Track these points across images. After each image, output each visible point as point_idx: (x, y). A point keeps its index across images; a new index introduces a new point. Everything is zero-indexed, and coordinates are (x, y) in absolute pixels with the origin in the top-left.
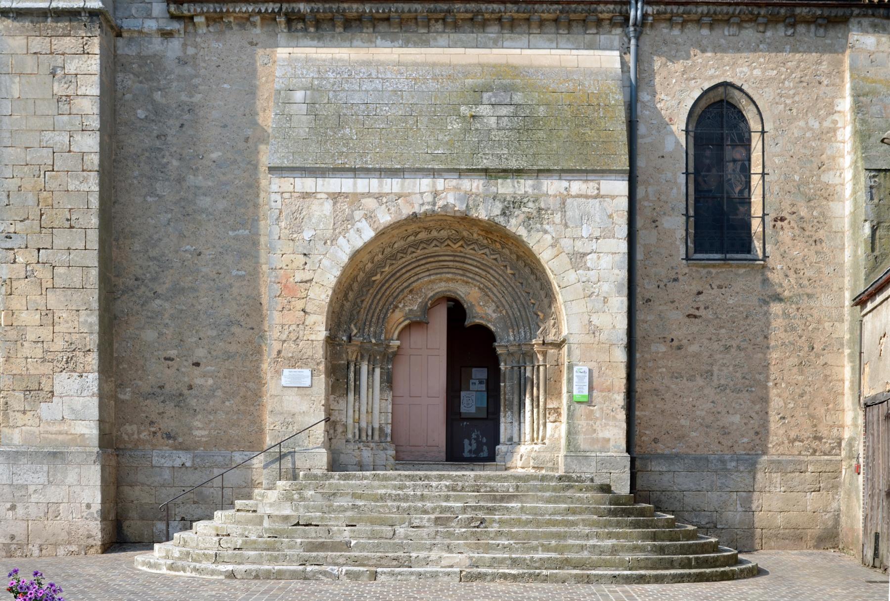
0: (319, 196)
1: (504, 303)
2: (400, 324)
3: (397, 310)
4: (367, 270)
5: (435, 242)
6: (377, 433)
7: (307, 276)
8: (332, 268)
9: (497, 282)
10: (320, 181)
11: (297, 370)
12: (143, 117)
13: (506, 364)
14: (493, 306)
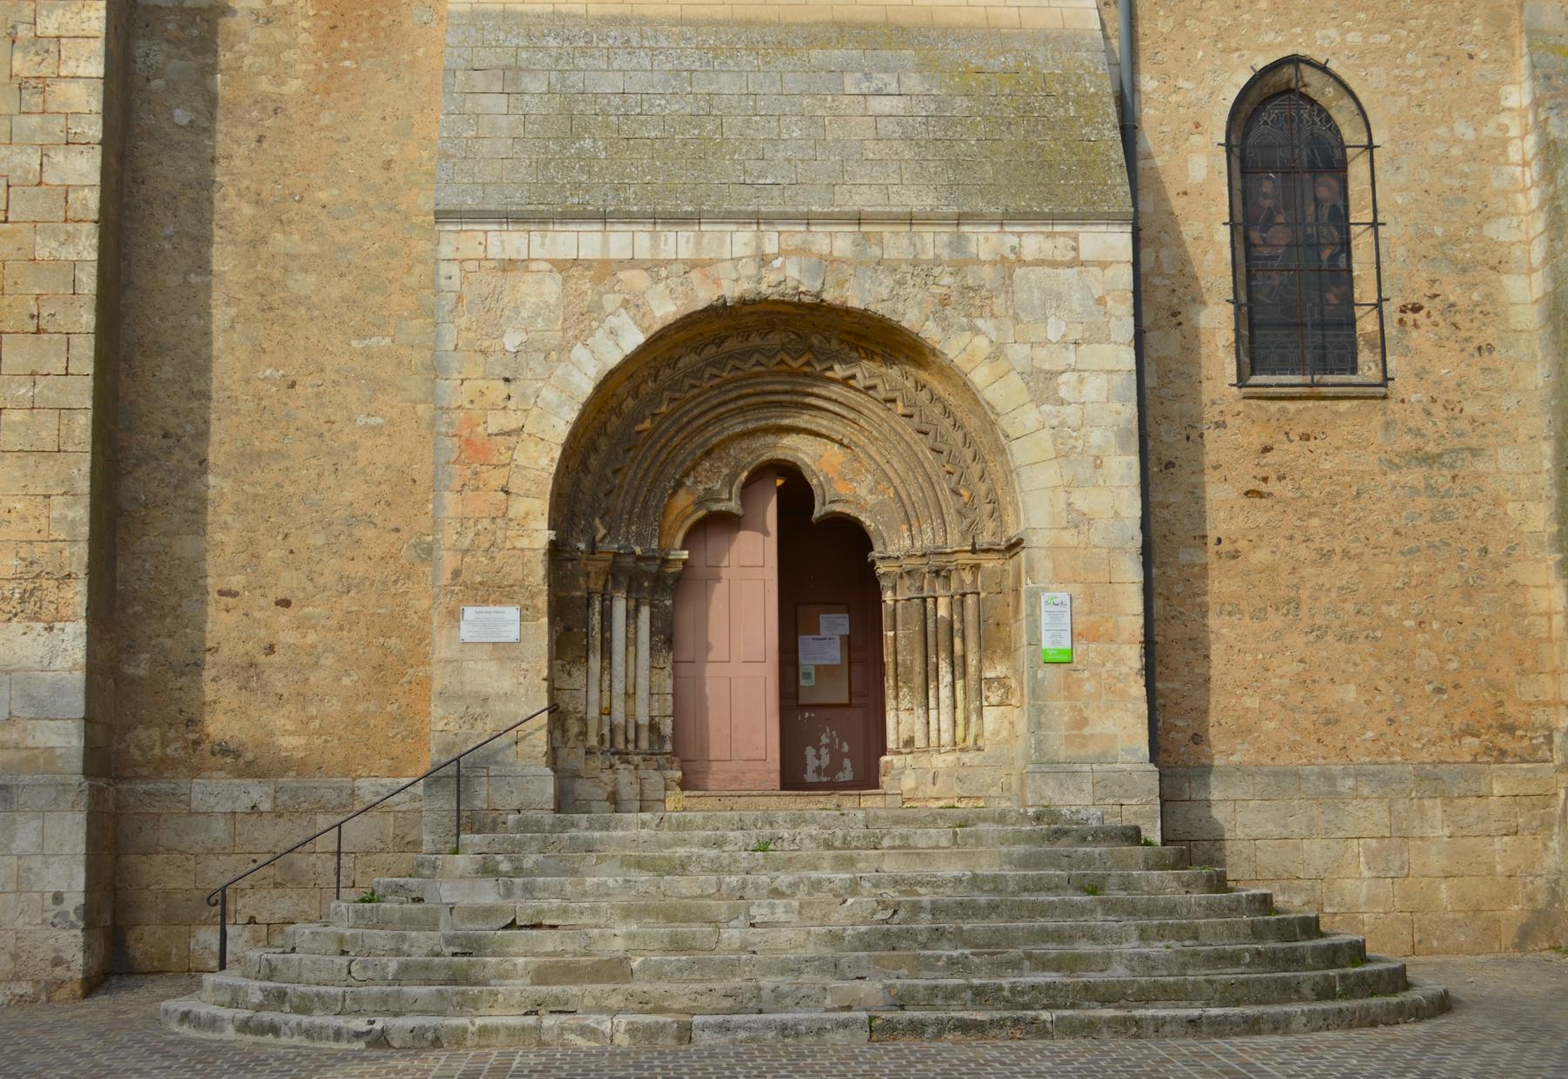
0: (534, 266)
2: (688, 517)
5: (756, 357)
6: (644, 735)
7: (512, 422)
8: (560, 405)
10: (536, 237)
11: (492, 608)
12: (185, 122)
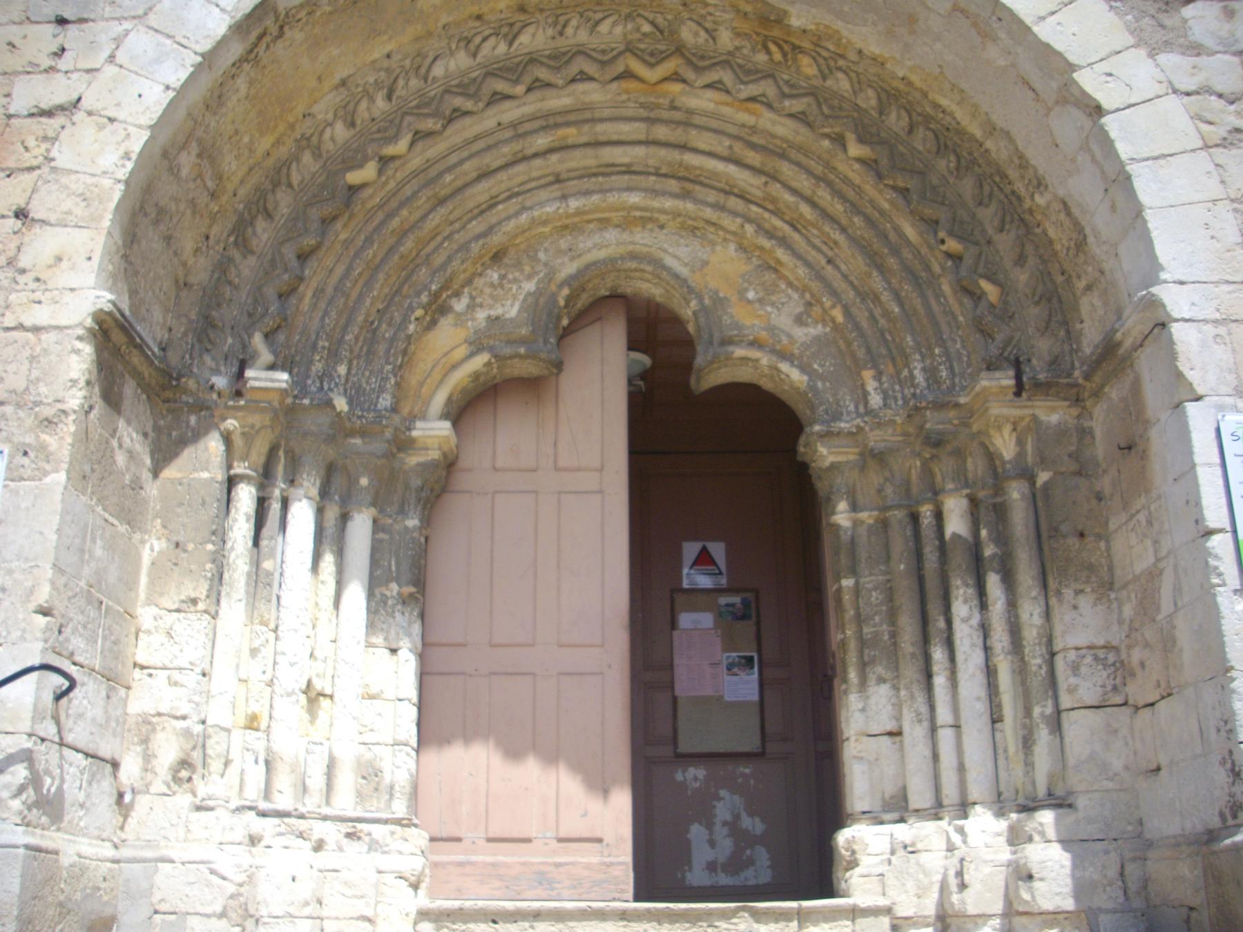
1: (840, 285)
2: (455, 367)
3: (445, 323)
4: (328, 146)
6: (346, 781)
7: (55, 91)
8: (158, 61)
9: (805, 209)
13: (854, 507)
14: (795, 304)
